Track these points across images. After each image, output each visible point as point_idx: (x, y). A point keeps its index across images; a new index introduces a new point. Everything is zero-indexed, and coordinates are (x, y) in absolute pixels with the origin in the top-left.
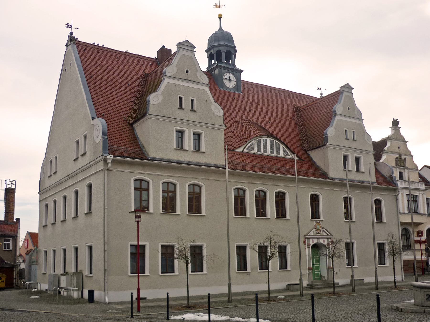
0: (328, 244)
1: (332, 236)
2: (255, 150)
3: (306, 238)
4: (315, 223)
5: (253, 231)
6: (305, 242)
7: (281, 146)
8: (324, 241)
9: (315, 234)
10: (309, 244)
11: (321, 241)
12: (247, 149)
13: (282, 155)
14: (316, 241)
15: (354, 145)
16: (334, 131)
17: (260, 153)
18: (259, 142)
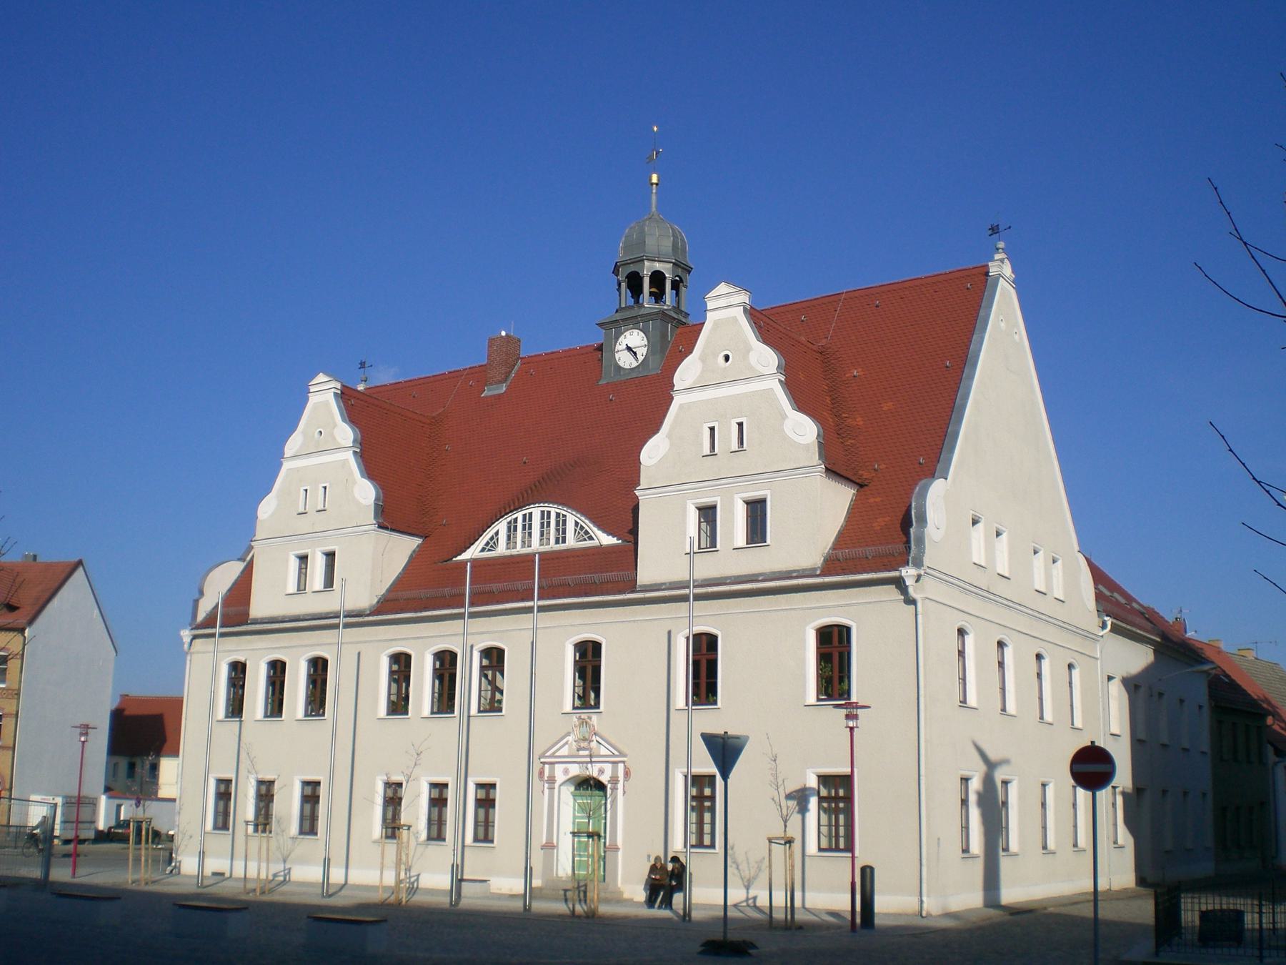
0: (614, 780)
1: (622, 754)
2: (501, 549)
3: (544, 763)
4: (574, 719)
5: (424, 748)
6: (541, 773)
7: (571, 518)
8: (601, 771)
9: (575, 753)
10: (552, 780)
11: (593, 771)
12: (483, 550)
13: (571, 542)
14: (575, 770)
15: (741, 464)
16: (667, 442)
17: (514, 552)
18: (512, 528)
